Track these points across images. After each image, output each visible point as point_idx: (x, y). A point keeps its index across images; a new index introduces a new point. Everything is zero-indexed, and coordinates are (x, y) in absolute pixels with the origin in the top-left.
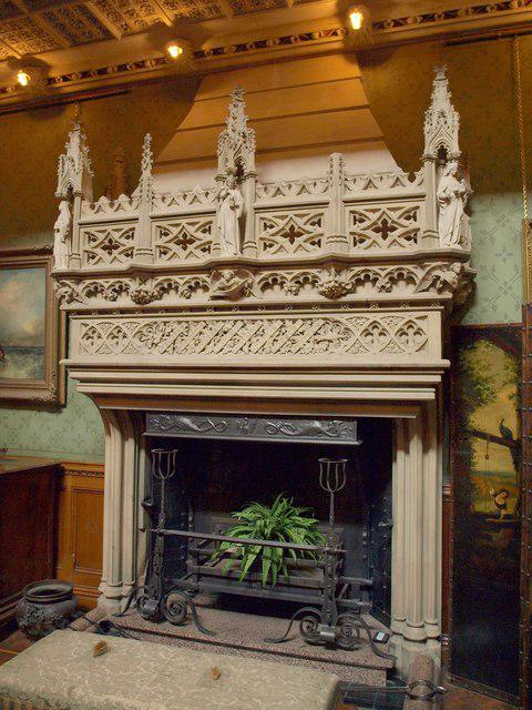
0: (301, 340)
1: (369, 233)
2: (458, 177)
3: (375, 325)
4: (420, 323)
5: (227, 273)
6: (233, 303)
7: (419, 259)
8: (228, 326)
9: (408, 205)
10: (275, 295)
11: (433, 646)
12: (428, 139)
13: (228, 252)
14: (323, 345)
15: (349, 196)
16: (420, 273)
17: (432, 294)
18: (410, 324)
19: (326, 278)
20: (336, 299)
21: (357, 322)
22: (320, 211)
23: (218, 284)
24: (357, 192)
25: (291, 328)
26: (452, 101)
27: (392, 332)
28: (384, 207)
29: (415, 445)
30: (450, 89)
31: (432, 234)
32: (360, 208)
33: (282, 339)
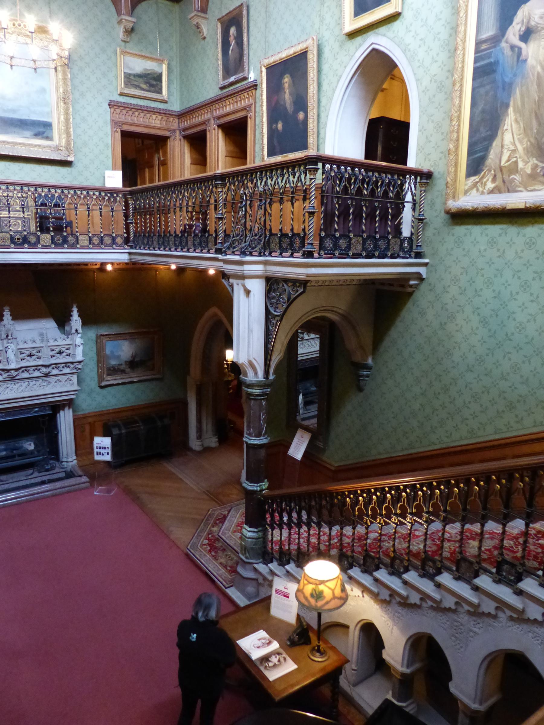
0: (35, 387)
1: (56, 355)
2: (81, 338)
3: (58, 380)
4: (71, 378)
5: (12, 371)
6: (13, 379)
7: (72, 363)
8: (8, 385)
9: (68, 346)
10: (26, 375)
11: (75, 462)
12: (73, 327)
13: (13, 366)
14: (42, 387)
15: (49, 344)
16: (72, 366)
17: (75, 371)
18: (68, 379)
19: (44, 370)
20: (47, 375)
21: (53, 380)
22: (40, 349)
23: (7, 374)
24: (52, 343)
25: (31, 384)
26: (79, 316)
27: (63, 381)
28: (60, 347)
29: (66, 409)
30: (78, 311)
31: (74, 356)
32: (53, 348)
33: (28, 387)
